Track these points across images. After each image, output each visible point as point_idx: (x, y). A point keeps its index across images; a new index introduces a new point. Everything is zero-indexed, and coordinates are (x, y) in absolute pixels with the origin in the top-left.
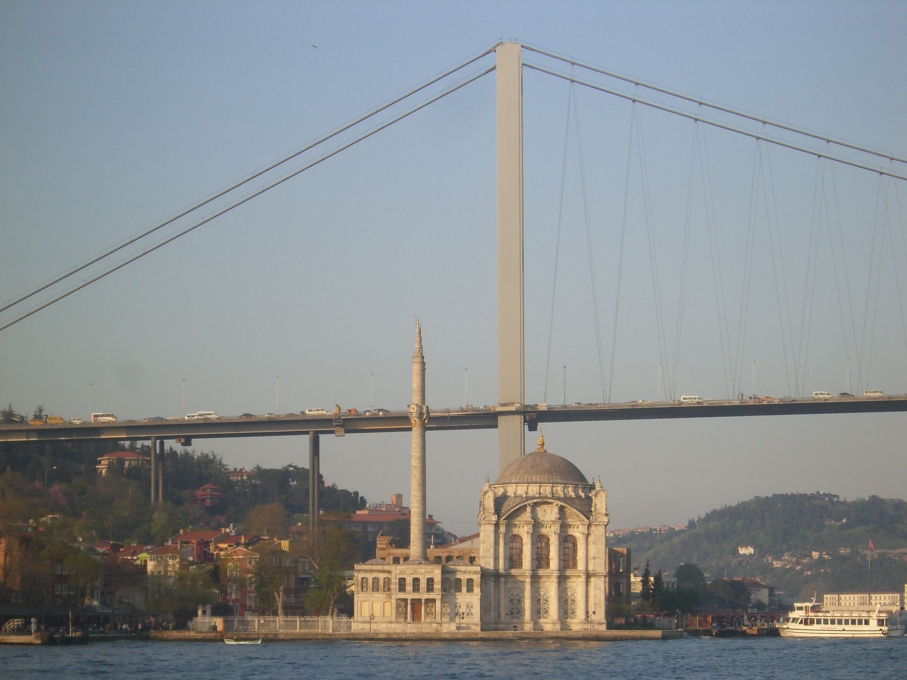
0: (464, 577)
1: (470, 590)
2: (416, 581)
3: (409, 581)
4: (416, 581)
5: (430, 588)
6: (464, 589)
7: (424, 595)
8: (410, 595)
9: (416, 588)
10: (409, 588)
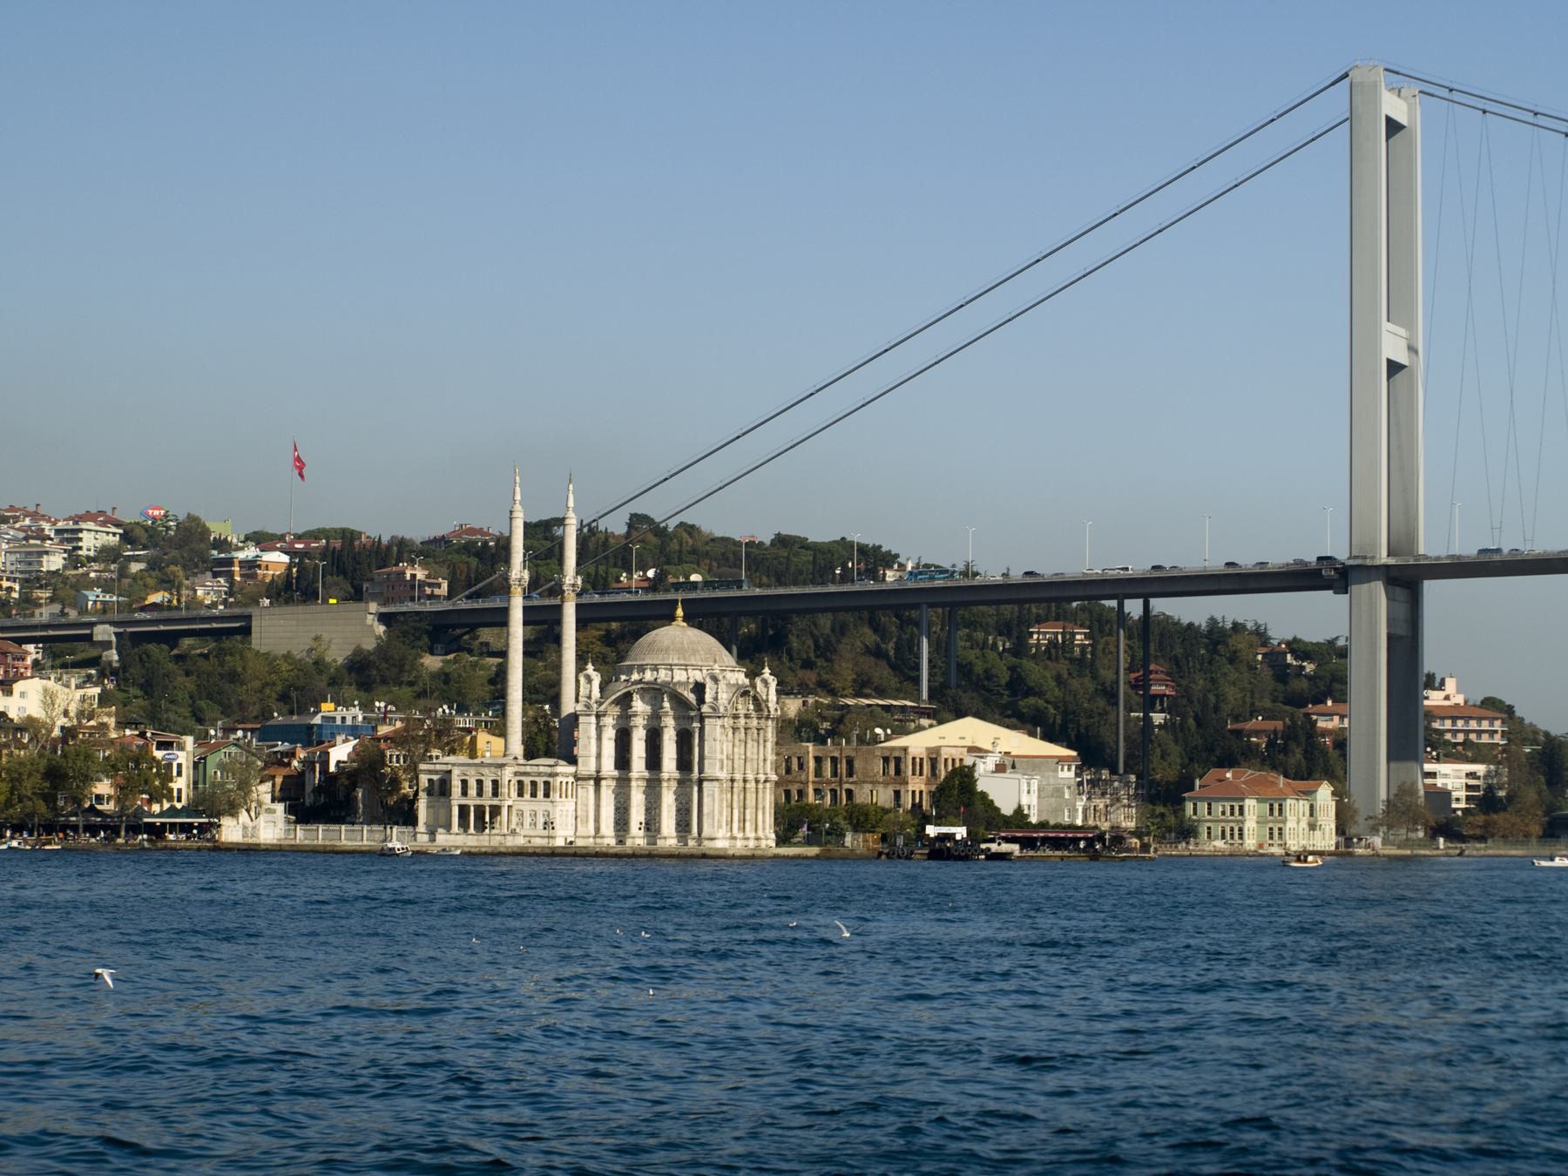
0: (540, 781)
1: (547, 795)
2: (480, 783)
3: (472, 784)
4: (480, 783)
5: (495, 793)
6: (540, 793)
7: (487, 801)
8: (472, 801)
9: (480, 793)
10: (473, 791)
